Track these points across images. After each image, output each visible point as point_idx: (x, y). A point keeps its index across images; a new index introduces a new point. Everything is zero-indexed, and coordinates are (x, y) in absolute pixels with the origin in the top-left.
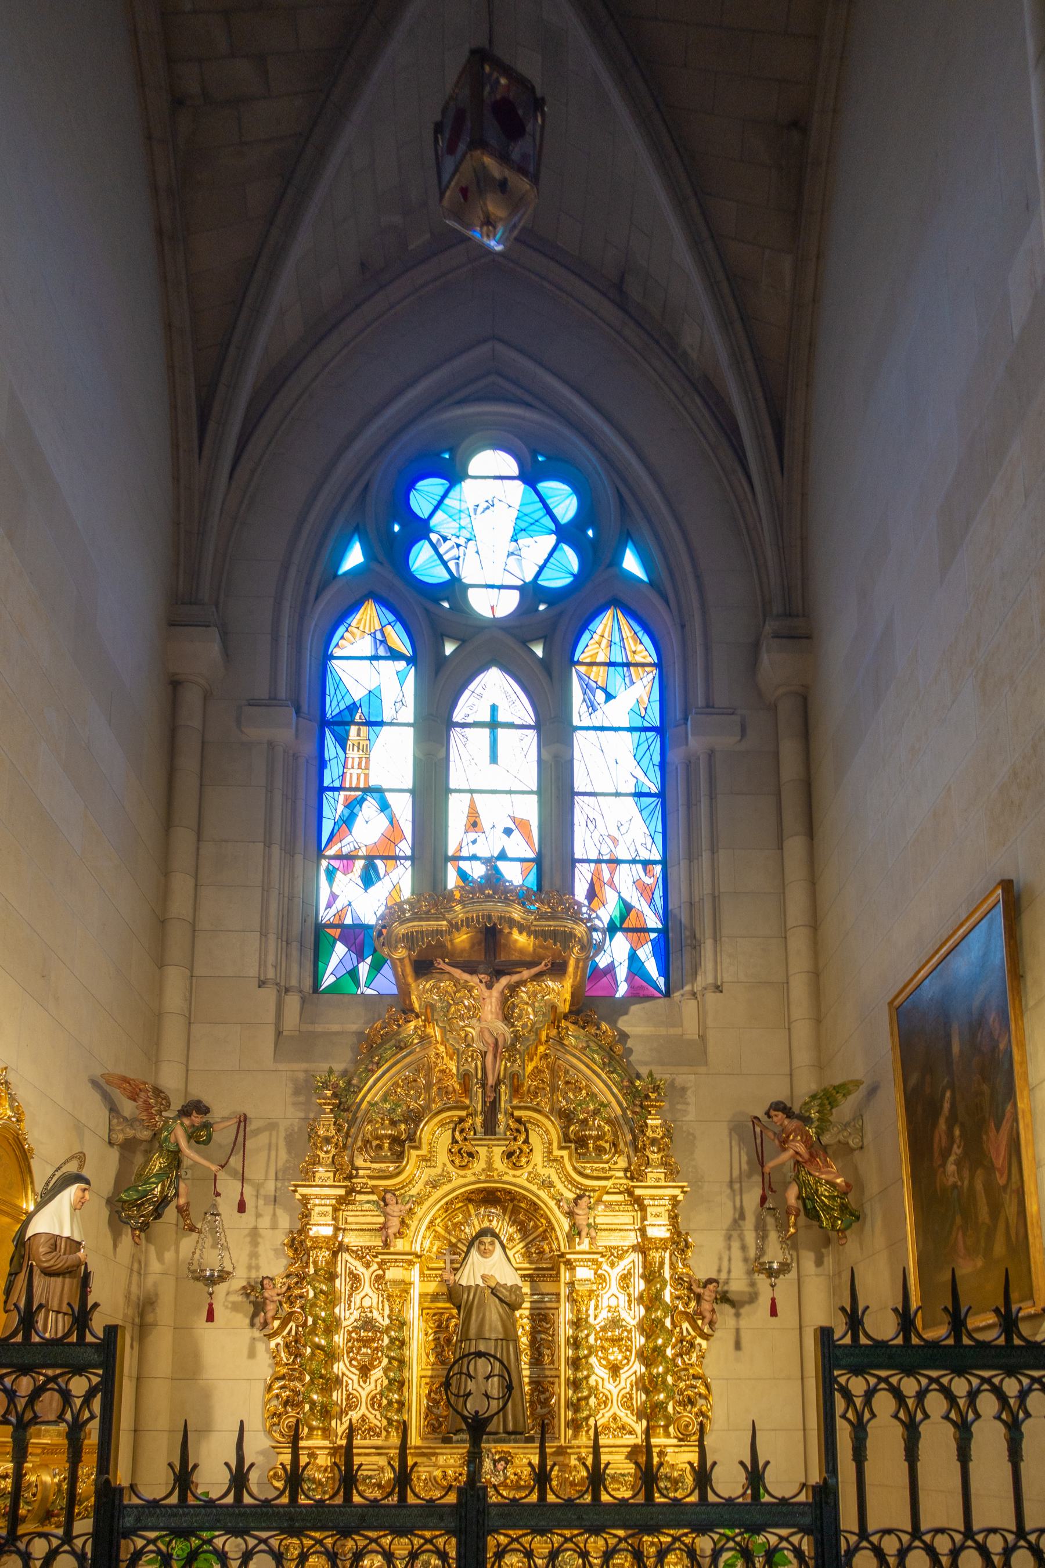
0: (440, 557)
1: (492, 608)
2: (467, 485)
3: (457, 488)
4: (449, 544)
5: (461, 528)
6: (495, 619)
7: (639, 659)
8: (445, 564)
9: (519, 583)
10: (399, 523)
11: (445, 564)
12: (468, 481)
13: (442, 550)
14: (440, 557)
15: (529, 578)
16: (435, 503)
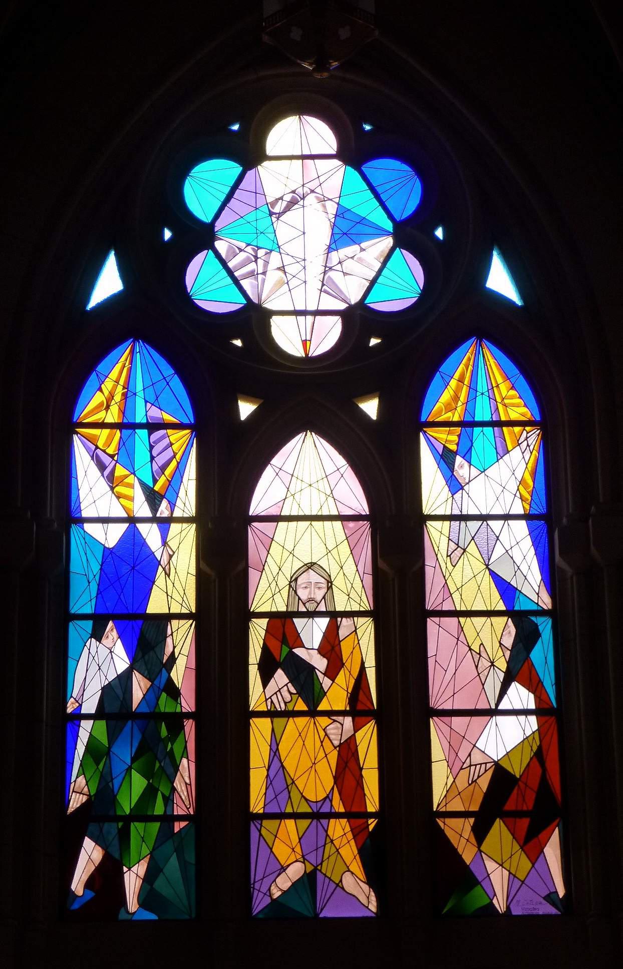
0: (230, 273)
1: (304, 343)
2: (265, 169)
3: (250, 174)
4: (242, 256)
5: (259, 233)
6: (308, 360)
7: (514, 415)
8: (236, 282)
9: (342, 306)
10: (170, 229)
11: (236, 282)
12: (266, 164)
13: (231, 265)
14: (230, 273)
15: (354, 299)
16: (223, 197)
